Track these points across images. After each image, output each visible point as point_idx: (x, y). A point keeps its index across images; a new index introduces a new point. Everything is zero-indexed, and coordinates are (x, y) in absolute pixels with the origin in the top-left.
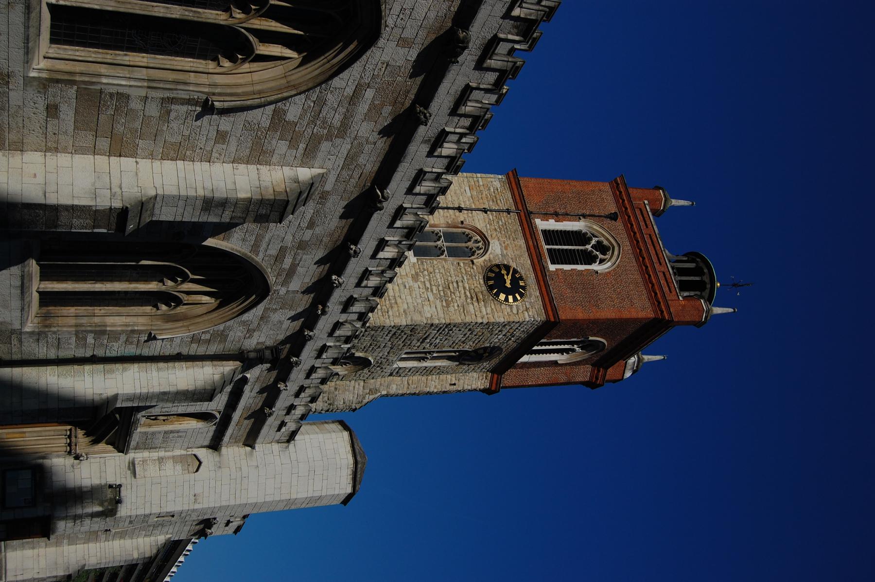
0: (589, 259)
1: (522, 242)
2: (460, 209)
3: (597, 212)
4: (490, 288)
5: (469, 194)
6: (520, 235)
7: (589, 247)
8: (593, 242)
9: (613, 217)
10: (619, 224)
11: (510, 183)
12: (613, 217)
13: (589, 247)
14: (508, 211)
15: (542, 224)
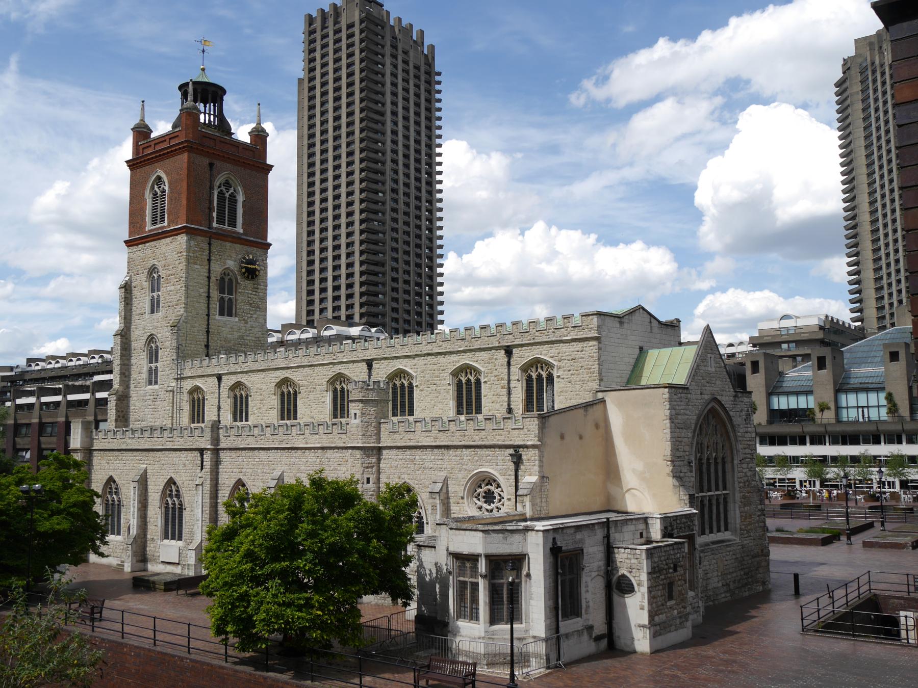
0: (233, 200)
1: (228, 244)
2: (209, 277)
3: (207, 176)
4: (253, 278)
5: (198, 267)
6: (223, 243)
7: (227, 195)
8: (223, 188)
9: (211, 165)
10: (217, 163)
11: (192, 234)
12: (211, 165)
13: (227, 195)
14: (210, 244)
15: (215, 225)
